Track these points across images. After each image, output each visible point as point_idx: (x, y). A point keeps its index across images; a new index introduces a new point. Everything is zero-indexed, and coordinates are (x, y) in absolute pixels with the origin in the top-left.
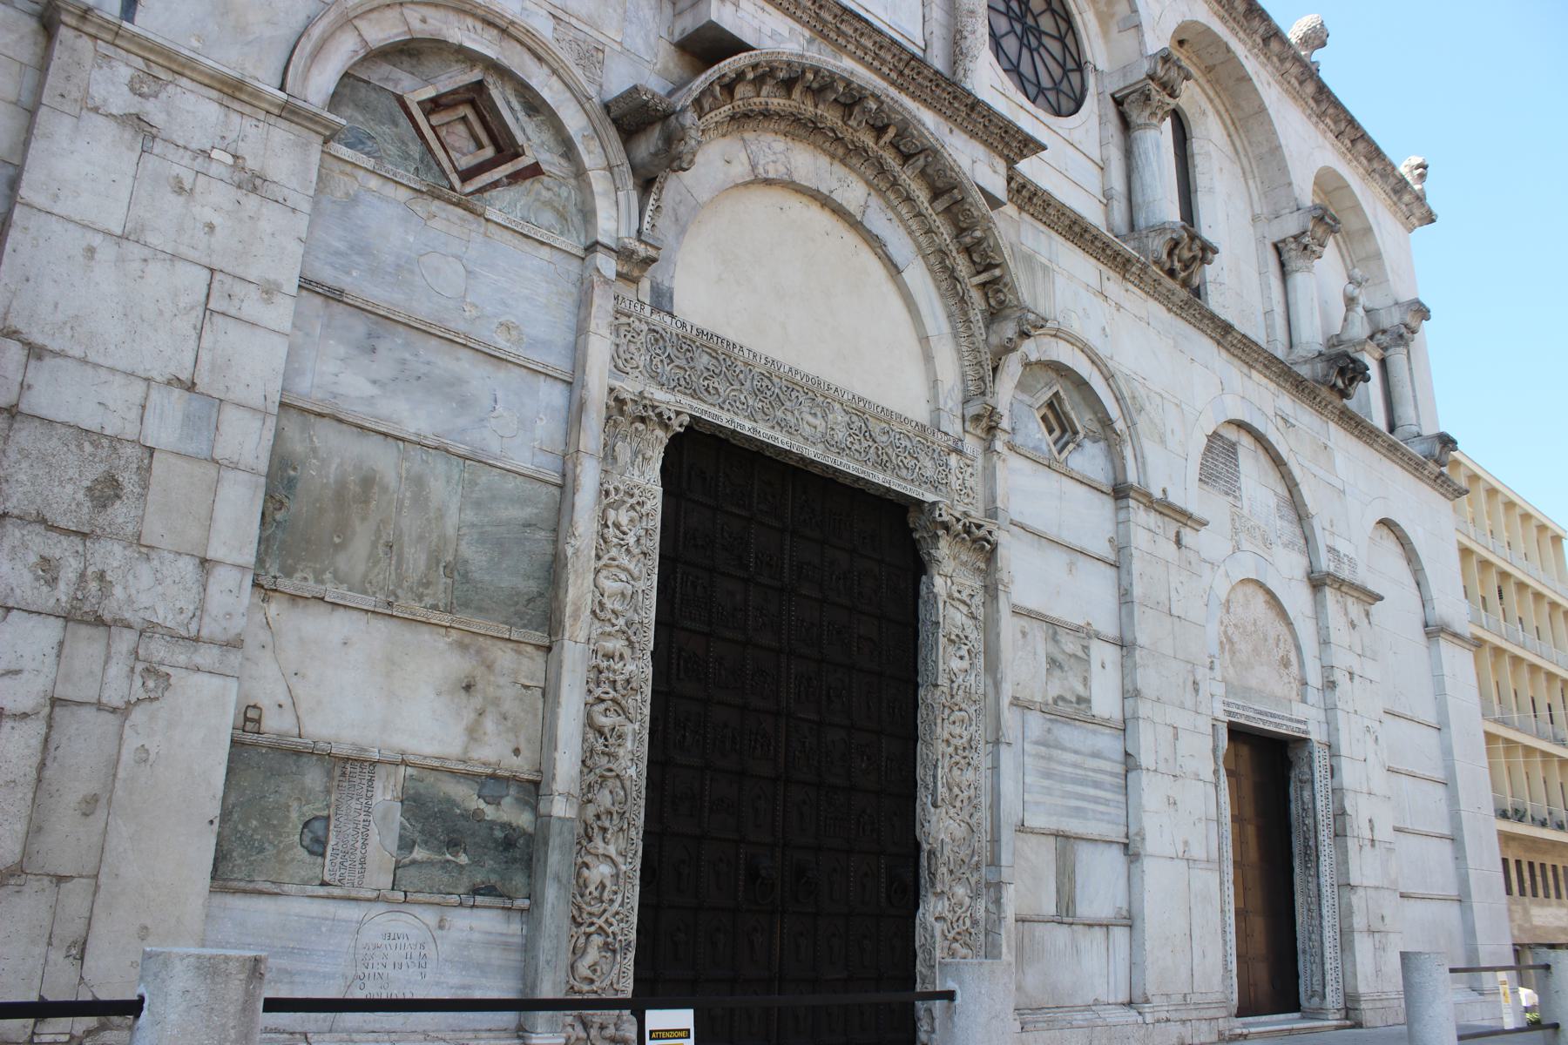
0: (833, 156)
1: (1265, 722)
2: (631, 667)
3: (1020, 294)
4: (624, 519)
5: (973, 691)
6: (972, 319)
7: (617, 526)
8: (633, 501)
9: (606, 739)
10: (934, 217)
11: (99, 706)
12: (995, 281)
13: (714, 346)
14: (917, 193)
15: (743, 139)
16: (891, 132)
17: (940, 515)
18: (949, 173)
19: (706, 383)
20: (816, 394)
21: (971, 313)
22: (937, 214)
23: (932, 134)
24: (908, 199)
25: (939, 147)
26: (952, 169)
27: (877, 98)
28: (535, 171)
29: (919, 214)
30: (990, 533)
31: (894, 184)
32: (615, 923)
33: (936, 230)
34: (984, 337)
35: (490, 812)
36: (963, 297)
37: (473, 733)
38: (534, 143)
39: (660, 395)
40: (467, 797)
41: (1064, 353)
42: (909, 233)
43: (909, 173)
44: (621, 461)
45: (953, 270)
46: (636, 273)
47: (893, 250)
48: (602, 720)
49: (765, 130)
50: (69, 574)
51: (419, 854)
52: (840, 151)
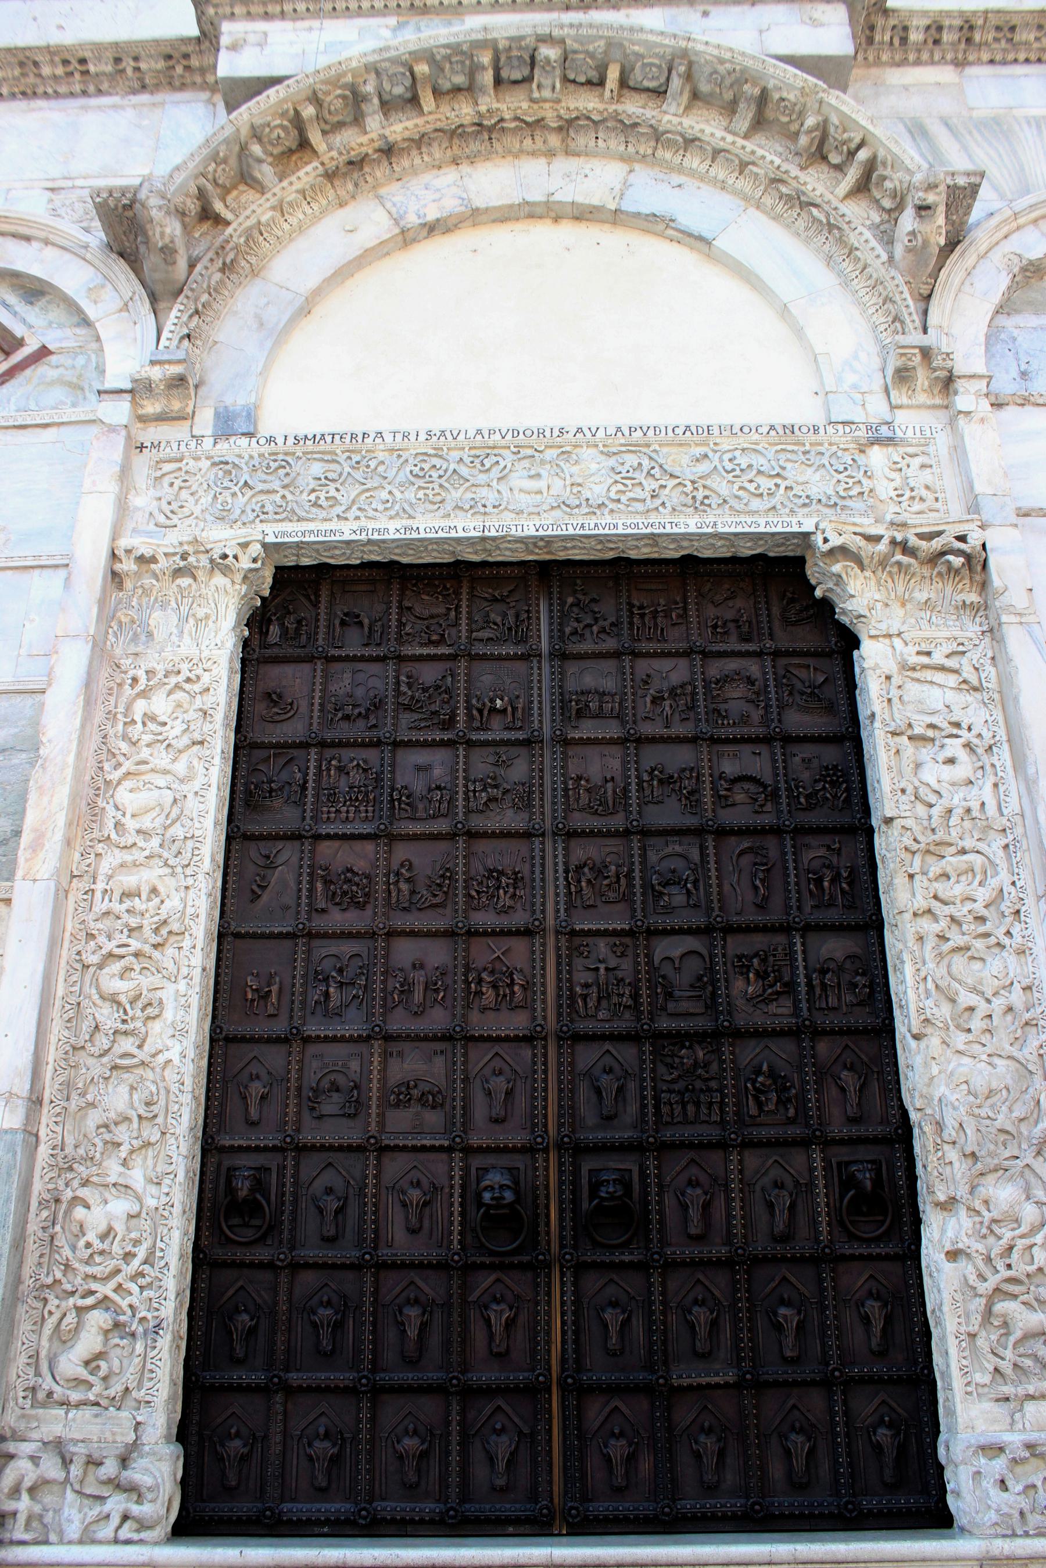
0: (551, 154)
3: (907, 162)
5: (991, 810)
6: (856, 245)
7: (149, 717)
8: (180, 678)
9: (125, 1012)
10: (740, 142)
12: (870, 167)
13: (328, 448)
14: (697, 127)
15: (379, 197)
16: (613, 75)
17: (826, 540)
18: (721, 69)
19: (312, 497)
21: (853, 239)
22: (746, 137)
23: (662, 33)
24: (690, 142)
25: (683, 44)
26: (722, 61)
27: (547, 39)
28: (44, 352)
29: (717, 152)
31: (657, 136)
32: (134, 1288)
33: (753, 158)
34: (884, 257)
36: (829, 223)
42: (723, 188)
43: (673, 109)
44: (159, 636)
45: (799, 194)
46: (176, 405)
47: (687, 221)
49: (414, 171)
52: (554, 140)
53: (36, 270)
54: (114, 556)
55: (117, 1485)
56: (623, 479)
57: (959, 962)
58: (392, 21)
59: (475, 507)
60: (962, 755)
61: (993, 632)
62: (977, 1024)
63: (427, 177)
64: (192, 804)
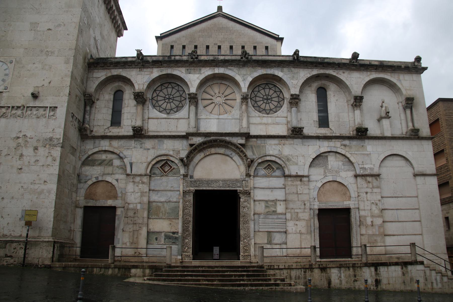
1: (332, 207)
2: (190, 219)
4: (188, 203)
7: (187, 204)
11: (136, 230)
20: (217, 181)
27: (218, 140)
30: (249, 191)
35: (174, 235)
37: (171, 229)
38: (174, 166)
39: (191, 188)
40: (171, 234)
41: (268, 158)
44: (187, 197)
48: (187, 225)
50: (133, 221)
51: (166, 240)
53: (173, 160)
54: (183, 191)
55: (189, 257)
56: (223, 184)
57: (244, 225)
58: (204, 137)
59: (211, 187)
60: (247, 209)
61: (250, 199)
62: (245, 229)
63: (207, 149)
64: (191, 211)
